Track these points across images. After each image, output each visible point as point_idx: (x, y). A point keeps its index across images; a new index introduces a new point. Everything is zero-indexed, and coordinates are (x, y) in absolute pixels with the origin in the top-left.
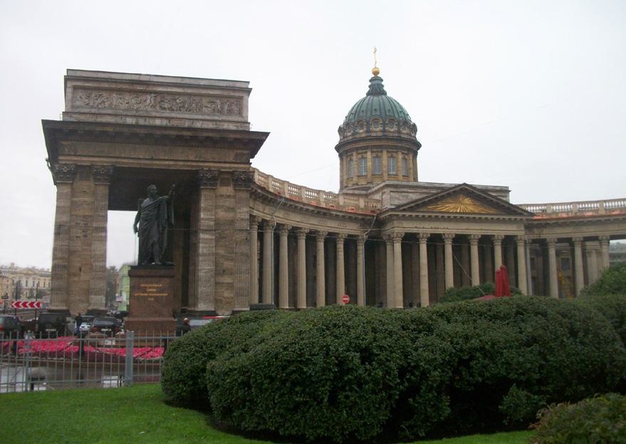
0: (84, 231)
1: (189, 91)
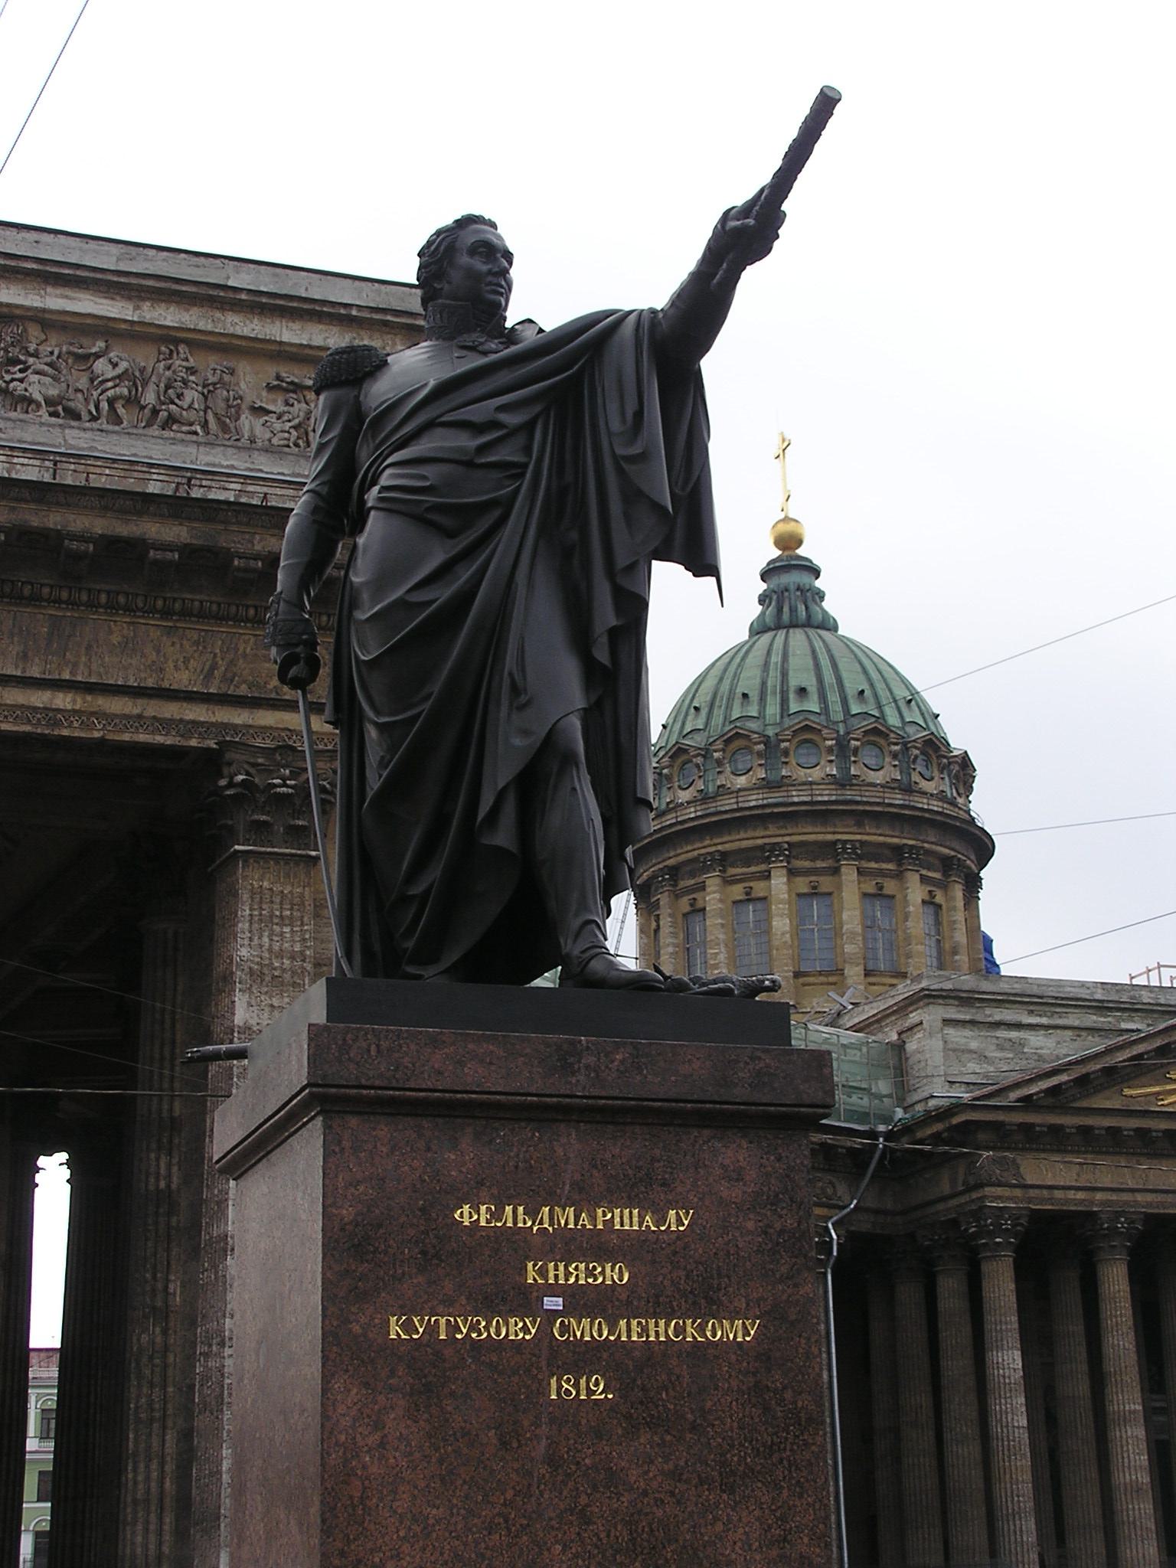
1: (169, 316)
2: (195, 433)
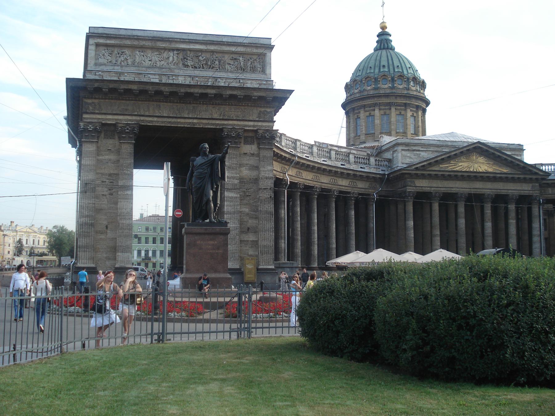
0: (110, 190)
1: (212, 48)
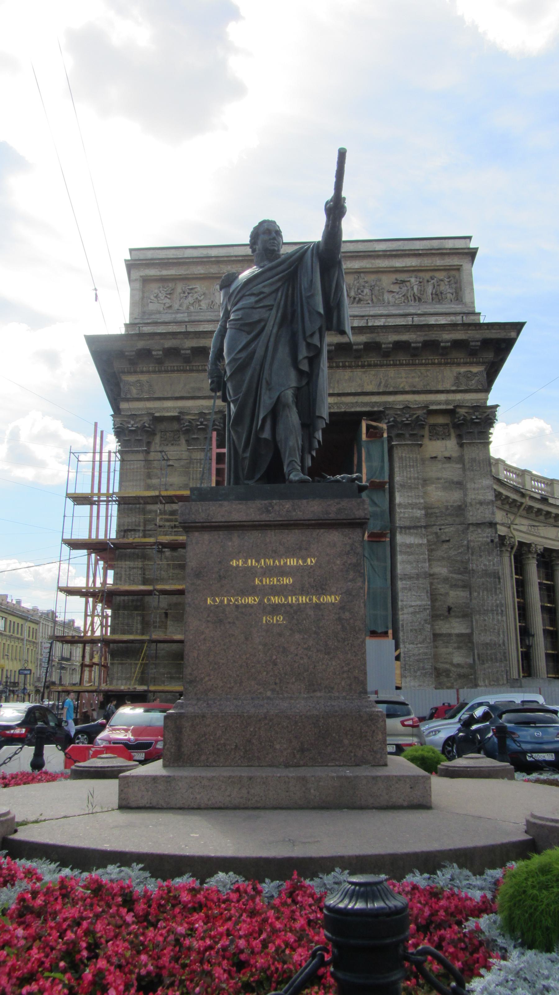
2: (369, 303)
